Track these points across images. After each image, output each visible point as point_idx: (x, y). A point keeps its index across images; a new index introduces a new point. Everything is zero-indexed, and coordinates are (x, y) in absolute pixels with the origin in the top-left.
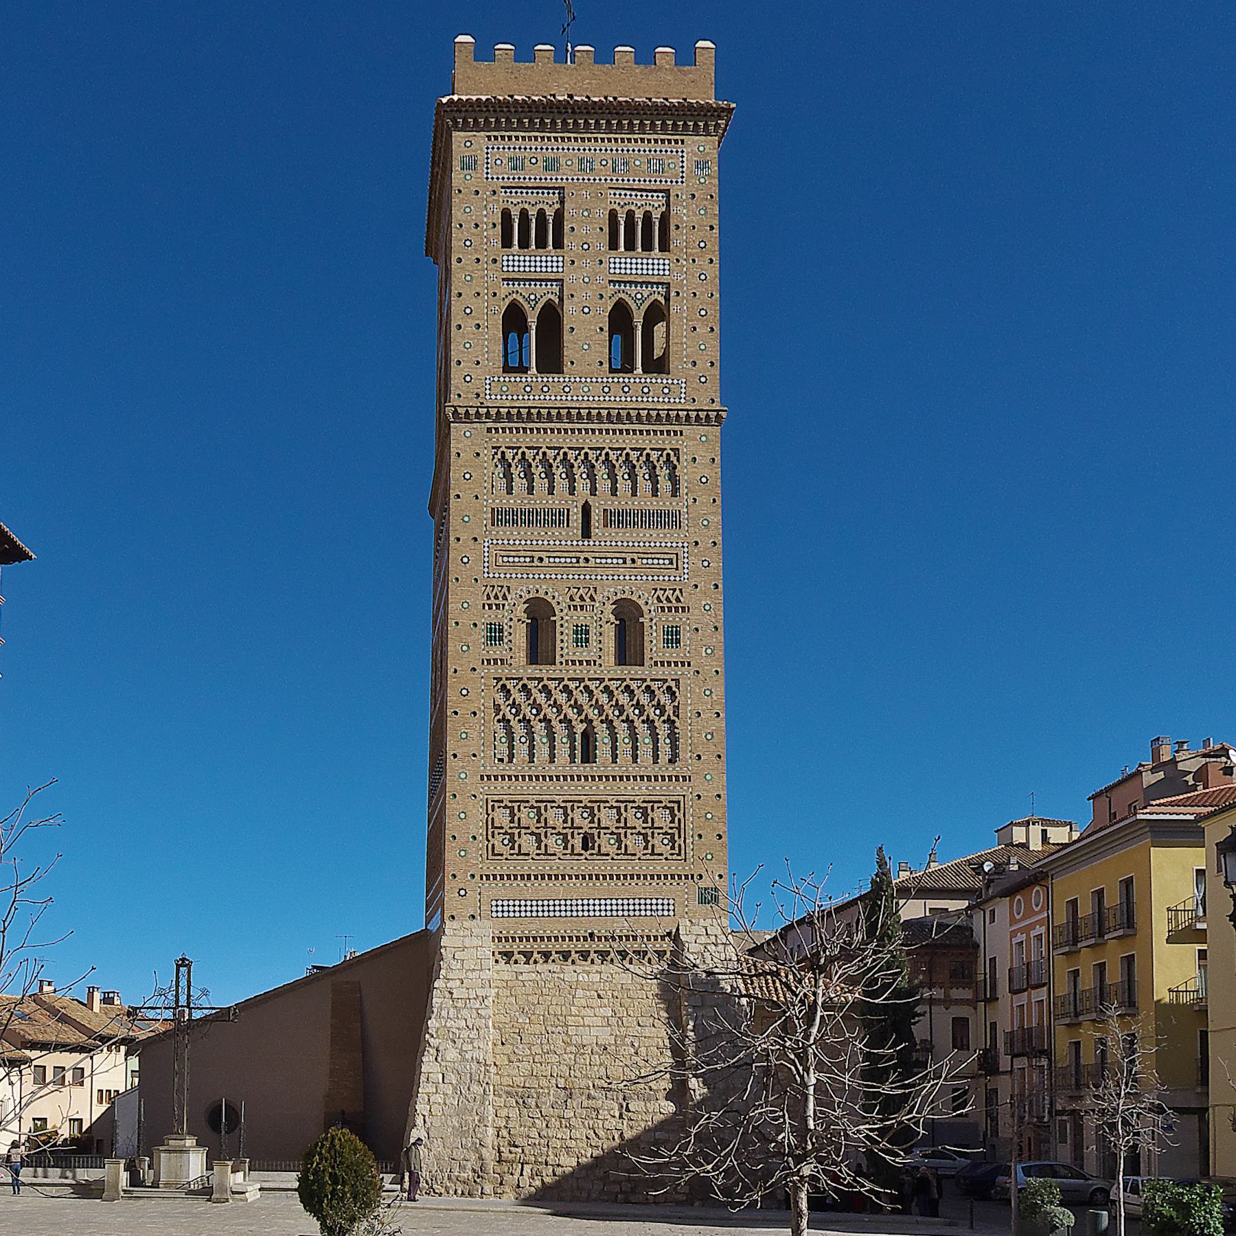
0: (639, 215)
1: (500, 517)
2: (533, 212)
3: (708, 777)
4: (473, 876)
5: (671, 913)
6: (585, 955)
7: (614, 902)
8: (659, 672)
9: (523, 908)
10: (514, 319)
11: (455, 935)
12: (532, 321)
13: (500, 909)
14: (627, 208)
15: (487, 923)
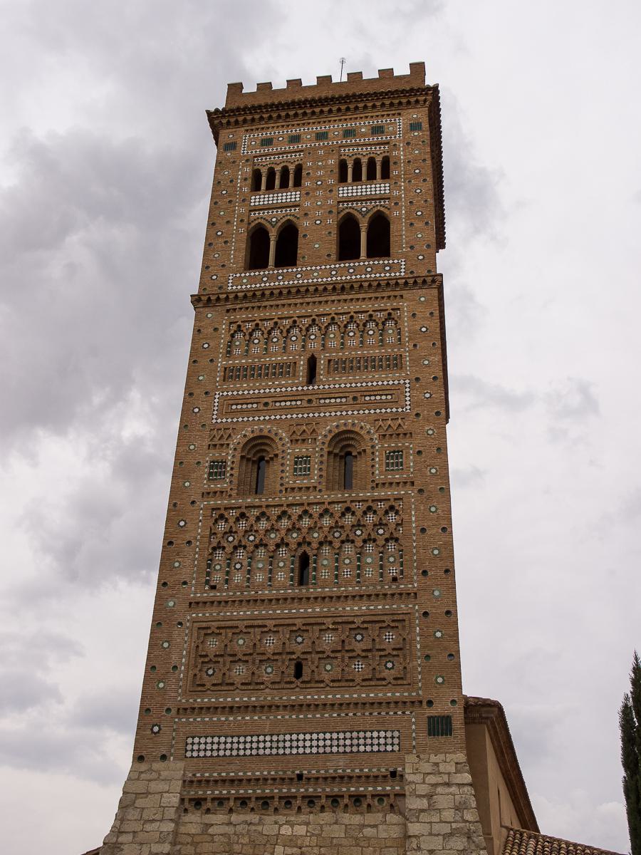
0: (364, 160)
1: (231, 374)
2: (278, 168)
3: (437, 593)
4: (168, 710)
5: (396, 748)
6: (288, 801)
7: (328, 736)
8: (382, 493)
9: (222, 746)
10: (258, 237)
11: (138, 779)
13: (196, 747)
14: (355, 157)
15: (181, 765)
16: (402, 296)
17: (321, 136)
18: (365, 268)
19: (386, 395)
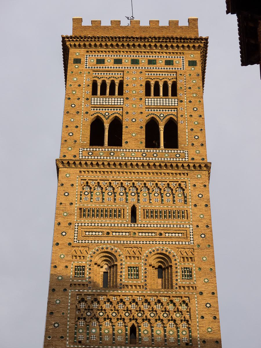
10: (97, 126)
12: (107, 126)
16: (187, 174)
17: (135, 62)
18: (163, 154)
19: (179, 233)
